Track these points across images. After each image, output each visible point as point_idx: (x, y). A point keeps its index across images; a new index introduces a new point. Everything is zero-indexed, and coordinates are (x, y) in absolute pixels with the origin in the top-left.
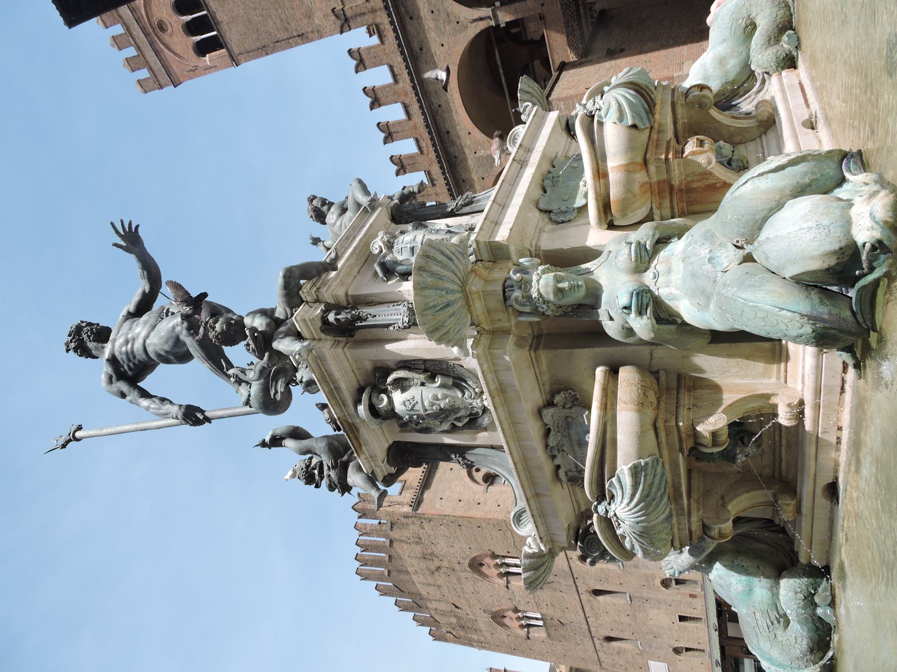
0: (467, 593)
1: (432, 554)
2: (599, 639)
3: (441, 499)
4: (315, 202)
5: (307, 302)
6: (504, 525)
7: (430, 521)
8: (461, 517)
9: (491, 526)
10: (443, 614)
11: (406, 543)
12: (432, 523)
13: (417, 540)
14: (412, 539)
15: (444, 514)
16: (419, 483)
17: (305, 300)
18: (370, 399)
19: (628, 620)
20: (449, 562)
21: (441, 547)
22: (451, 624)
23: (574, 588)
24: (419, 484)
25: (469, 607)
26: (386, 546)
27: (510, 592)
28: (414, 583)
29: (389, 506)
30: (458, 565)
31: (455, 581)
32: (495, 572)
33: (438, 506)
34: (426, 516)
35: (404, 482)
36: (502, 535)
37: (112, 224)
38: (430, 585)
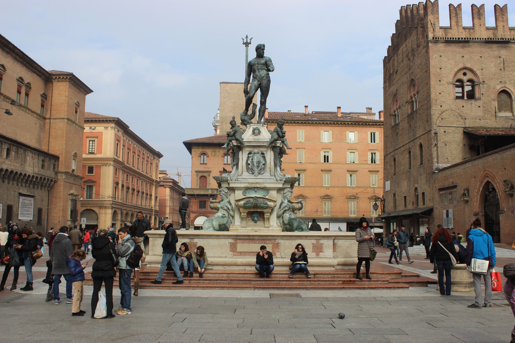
0: (402, 79)
1: (414, 55)
2: (394, 155)
3: (440, 56)
6: (429, 99)
8: (430, 72)
10: (393, 65)
12: (426, 53)
13: (419, 45)
19: (402, 170)
21: (418, 61)
22: (390, 70)
23: (410, 141)
24: (449, 39)
25: (397, 80)
31: (406, 71)
32: (412, 94)
33: (435, 56)
34: (428, 50)
38: (403, 54)
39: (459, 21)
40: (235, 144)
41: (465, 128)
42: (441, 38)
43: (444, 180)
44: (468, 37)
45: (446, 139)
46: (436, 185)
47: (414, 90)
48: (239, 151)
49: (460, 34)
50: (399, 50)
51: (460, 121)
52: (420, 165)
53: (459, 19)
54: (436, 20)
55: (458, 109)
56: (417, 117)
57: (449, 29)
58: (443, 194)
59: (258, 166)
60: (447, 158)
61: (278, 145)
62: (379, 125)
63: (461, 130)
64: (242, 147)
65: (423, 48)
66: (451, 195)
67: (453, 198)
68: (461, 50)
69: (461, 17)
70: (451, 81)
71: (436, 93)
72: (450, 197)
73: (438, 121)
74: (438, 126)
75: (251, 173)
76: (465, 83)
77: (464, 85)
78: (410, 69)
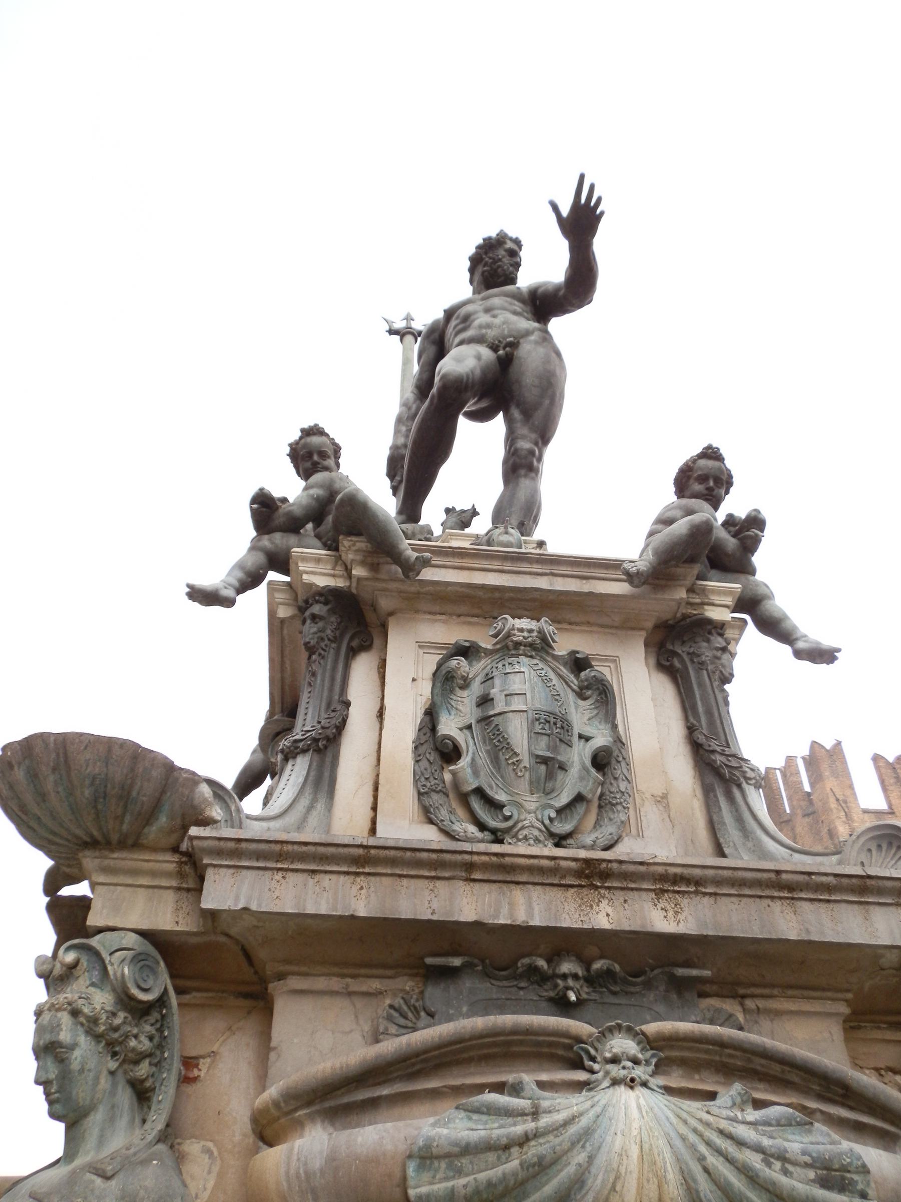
5: (340, 556)
29: (838, 800)
37: (582, 177)
40: (322, 582)
48: (353, 652)
54: (848, 792)
64: (391, 614)
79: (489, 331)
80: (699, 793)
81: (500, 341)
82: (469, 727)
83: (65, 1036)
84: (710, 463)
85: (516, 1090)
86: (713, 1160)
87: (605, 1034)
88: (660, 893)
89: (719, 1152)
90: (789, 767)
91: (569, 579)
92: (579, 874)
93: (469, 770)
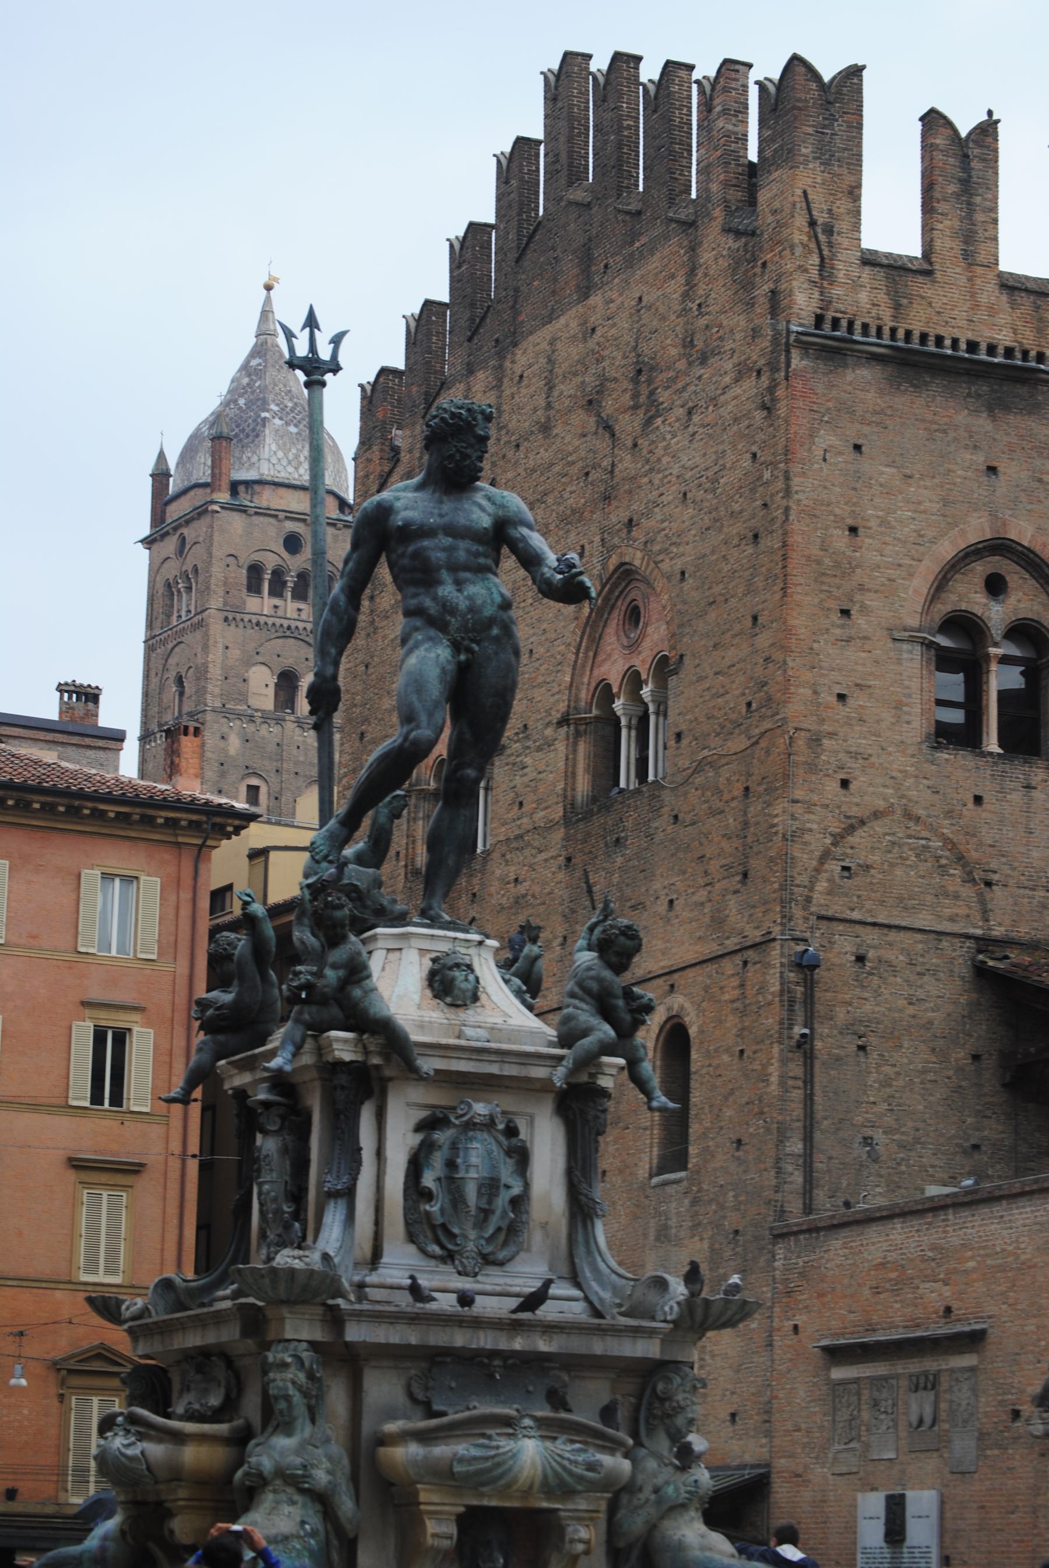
1: (653, 411)
3: (857, 448)
4: (622, 939)
6: (767, 725)
7: (764, 407)
8: (785, 545)
9: (759, 671)
11: (686, 296)
12: (759, 415)
13: (699, 344)
14: (703, 321)
15: (796, 468)
16: (924, 337)
17: (365, 1036)
18: (278, 1104)
20: (633, 479)
26: (671, 201)
27: (549, 732)
28: (550, 318)
30: (624, 515)
32: (613, 671)
33: (826, 439)
34: (780, 393)
35: (926, 266)
36: (733, 716)
38: (550, 387)
39: (981, 235)
40: (347, 1057)
41: (984, 944)
42: (865, 327)
43: (876, 1290)
44: (1028, 344)
45: (868, 1007)
46: (800, 1319)
47: (633, 647)
48: (362, 1103)
49: (982, 315)
50: (515, 344)
51: (957, 897)
52: (662, 1168)
53: (980, 217)
54: (842, 206)
55: (949, 814)
56: (650, 836)
57: (920, 279)
58: (856, 1381)
59: (485, 1213)
60: (867, 1141)
61: (606, 1082)
62: (172, 824)
63: (960, 955)
64: (390, 1079)
65: (742, 372)
66: (931, 1396)
67: (943, 1415)
68: (983, 423)
69: (994, 209)
70: (914, 622)
71: (815, 692)
72: (919, 1405)
73: (822, 886)
74: (821, 918)
75: (436, 1249)
76: (996, 645)
77: (987, 657)
78: (607, 498)
79: (453, 620)
80: (567, 1214)
81: (463, 638)
82: (439, 1179)
83: (291, 1392)
84: (628, 942)
85: (490, 1437)
86: (554, 1464)
87: (523, 1417)
88: (544, 1332)
89: (556, 1461)
90: (726, 90)
91: (513, 1066)
92: (509, 1324)
93: (438, 1213)
